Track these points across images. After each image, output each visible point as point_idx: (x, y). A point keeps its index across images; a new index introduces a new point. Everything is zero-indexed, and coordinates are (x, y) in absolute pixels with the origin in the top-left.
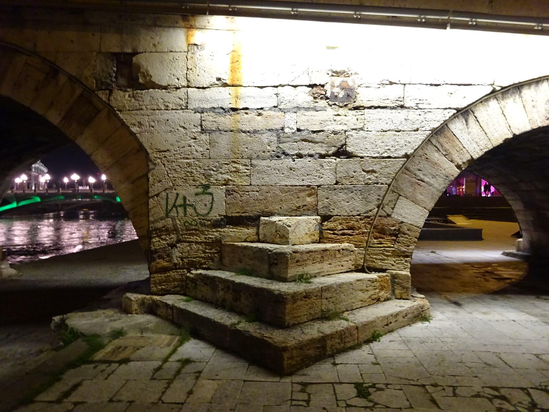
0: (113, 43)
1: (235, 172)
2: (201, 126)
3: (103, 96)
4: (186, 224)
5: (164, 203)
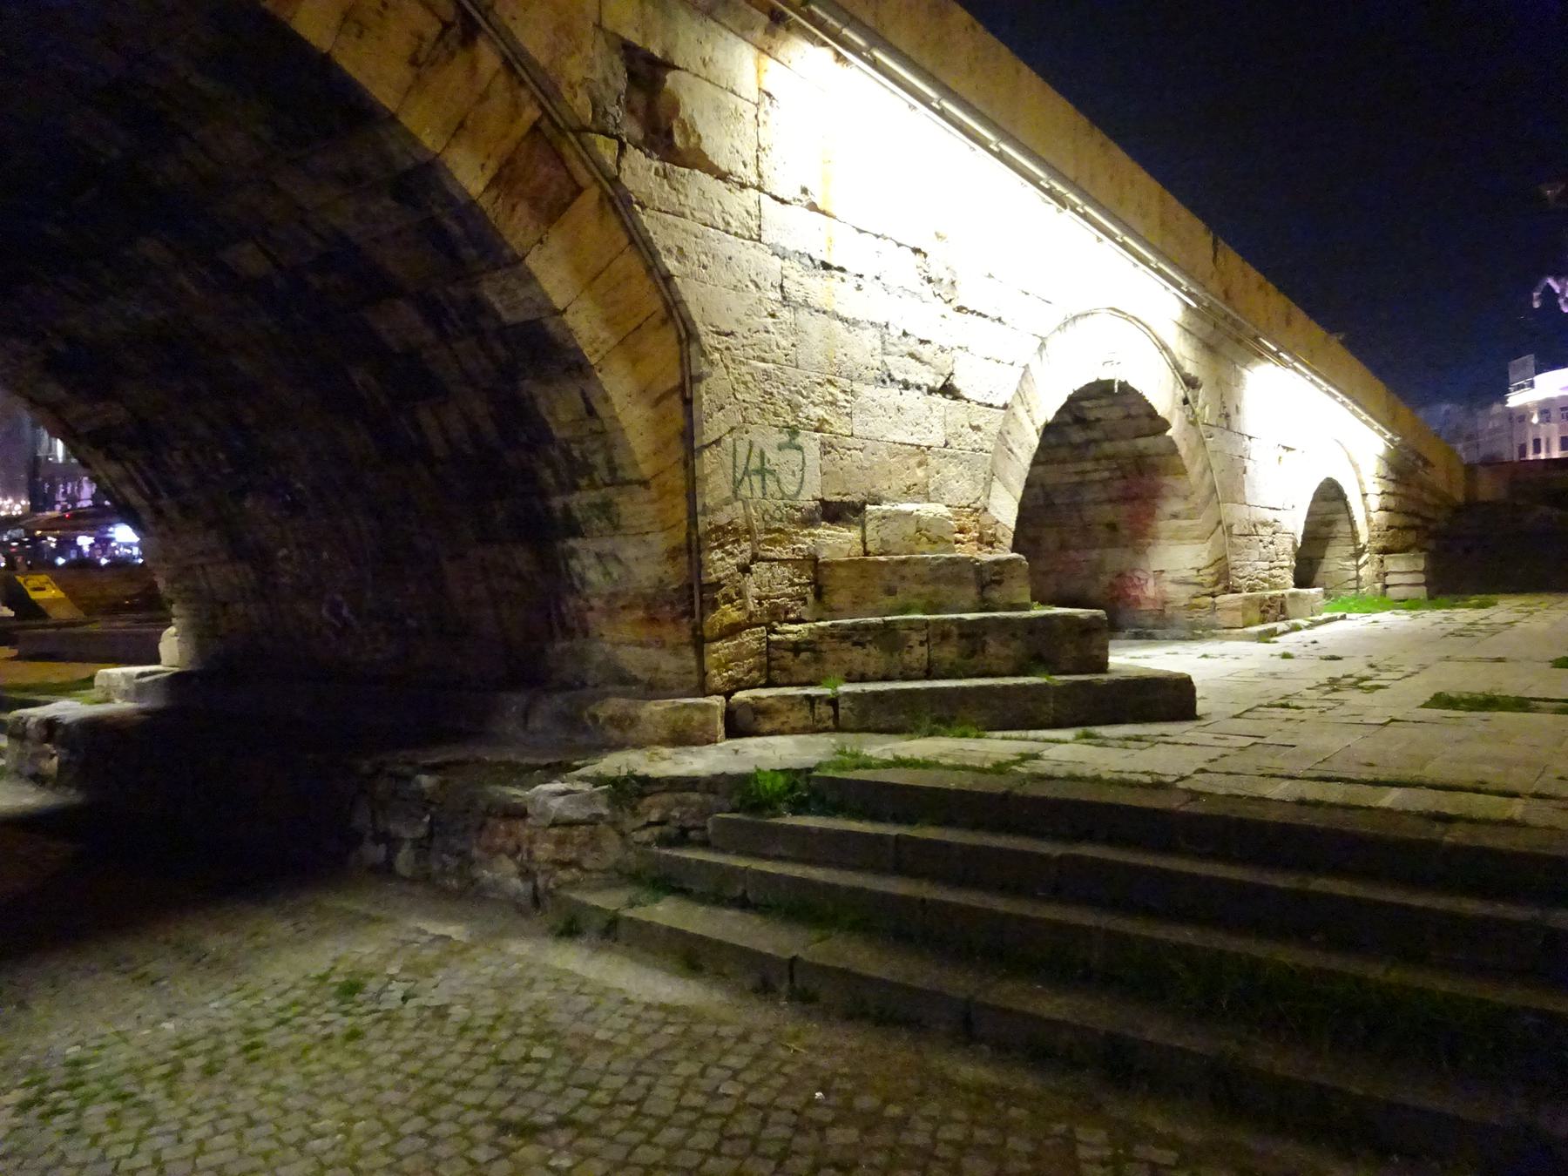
1: (832, 403)
2: (782, 287)
3: (606, 150)
4: (767, 517)
5: (729, 461)
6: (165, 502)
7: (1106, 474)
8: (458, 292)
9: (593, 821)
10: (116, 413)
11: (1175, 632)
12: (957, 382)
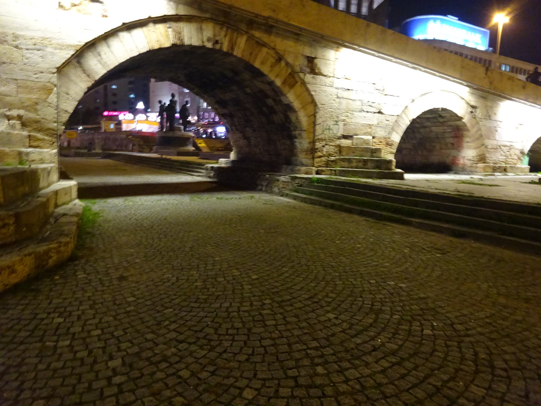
0: (308, 51)
3: (302, 75)
5: (322, 127)
6: (234, 128)
7: (449, 130)
8: (278, 98)
9: (288, 182)
10: (225, 111)
11: (465, 173)
12: (382, 111)
